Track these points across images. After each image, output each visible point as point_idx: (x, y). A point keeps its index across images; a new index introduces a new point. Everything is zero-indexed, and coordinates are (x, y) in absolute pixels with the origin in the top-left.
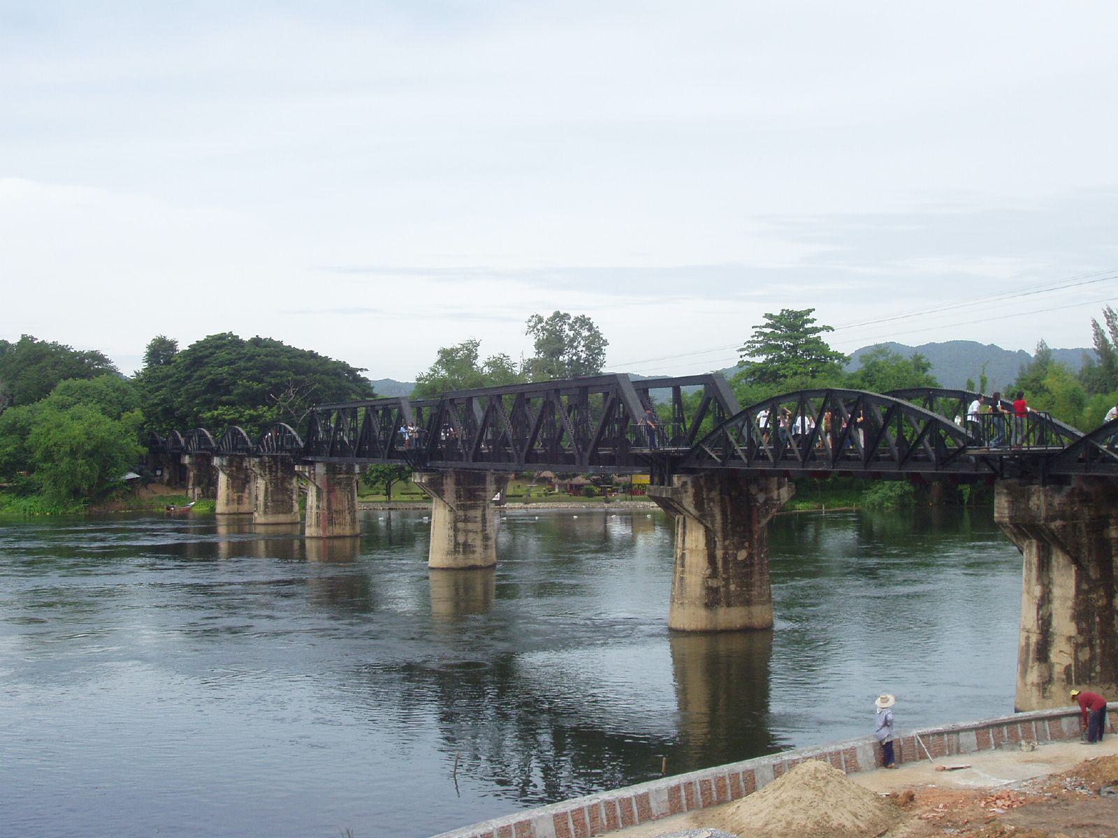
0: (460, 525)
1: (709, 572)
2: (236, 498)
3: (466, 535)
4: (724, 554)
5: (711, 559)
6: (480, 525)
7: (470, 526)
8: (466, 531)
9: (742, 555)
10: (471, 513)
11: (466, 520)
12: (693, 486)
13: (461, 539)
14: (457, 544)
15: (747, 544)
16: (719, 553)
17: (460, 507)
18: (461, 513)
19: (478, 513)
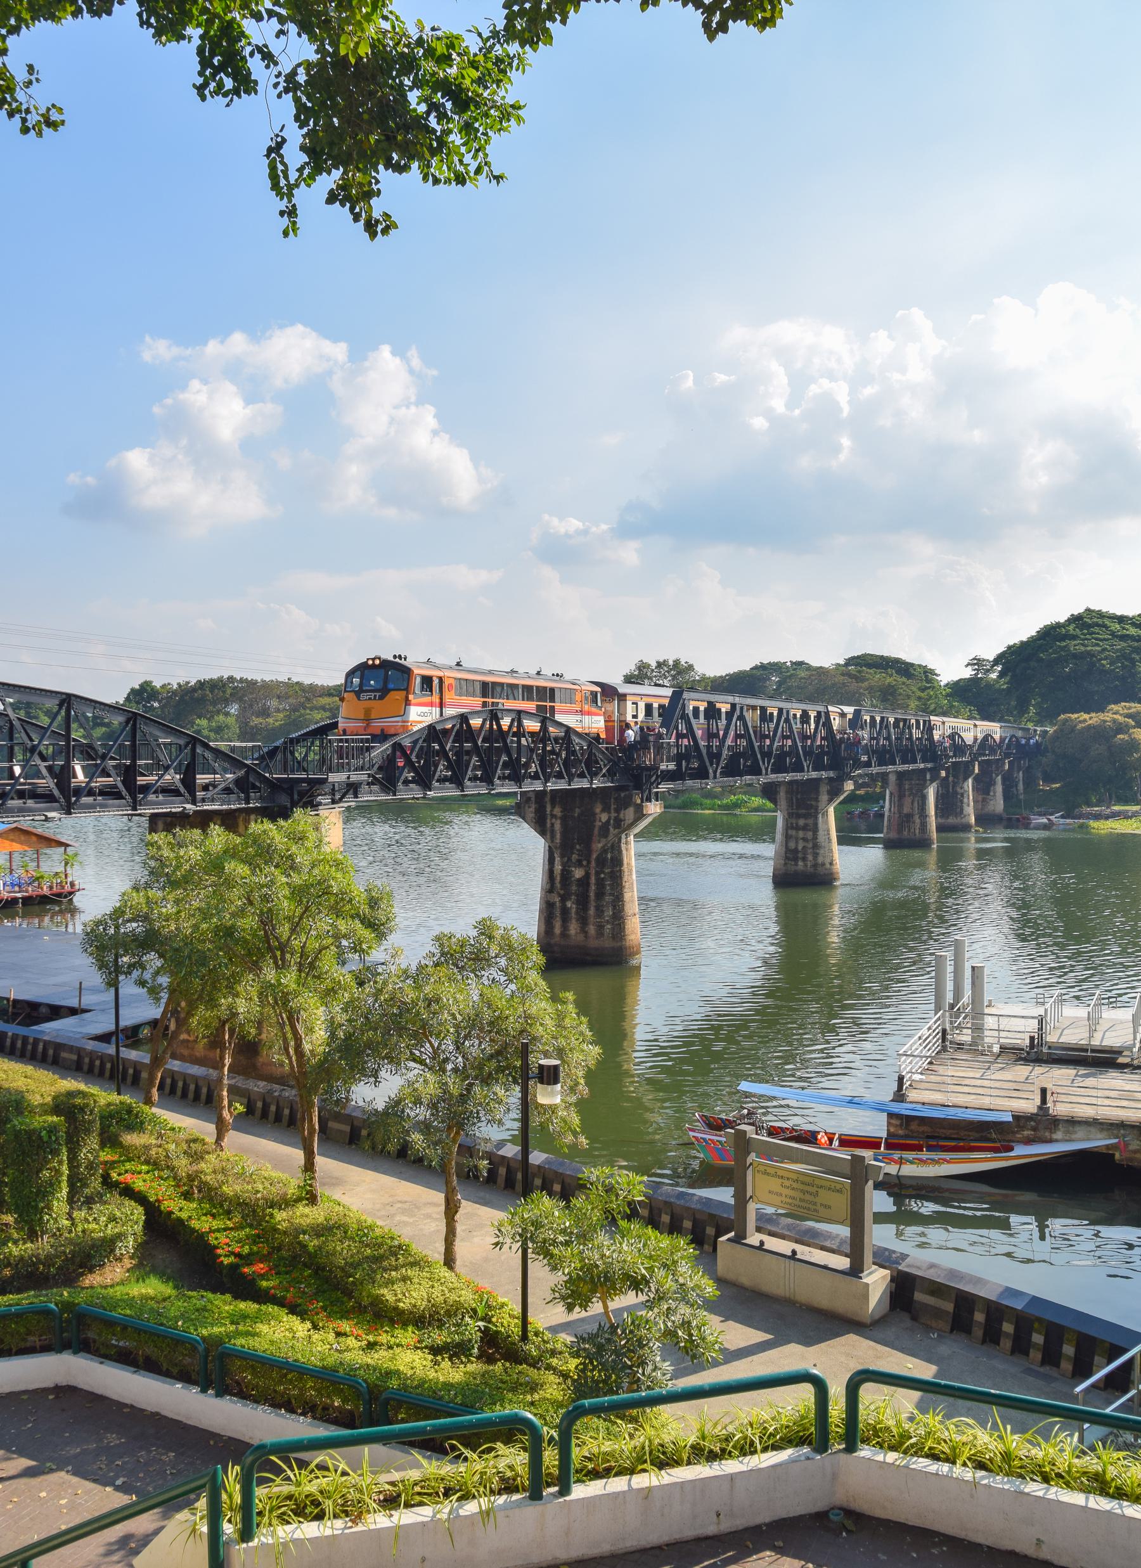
0: (792, 832)
1: (548, 887)
2: (980, 798)
3: (797, 842)
4: (562, 870)
5: (551, 873)
6: (811, 833)
7: (801, 834)
8: (797, 839)
9: (578, 873)
10: (801, 822)
11: (797, 828)
12: (536, 802)
13: (792, 845)
14: (788, 850)
15: (585, 863)
16: (558, 867)
17: (790, 815)
18: (794, 821)
19: (810, 821)
